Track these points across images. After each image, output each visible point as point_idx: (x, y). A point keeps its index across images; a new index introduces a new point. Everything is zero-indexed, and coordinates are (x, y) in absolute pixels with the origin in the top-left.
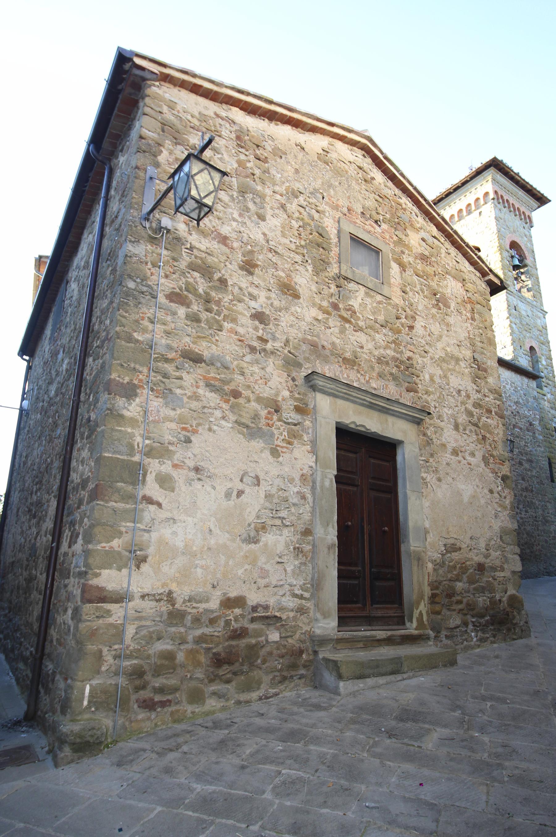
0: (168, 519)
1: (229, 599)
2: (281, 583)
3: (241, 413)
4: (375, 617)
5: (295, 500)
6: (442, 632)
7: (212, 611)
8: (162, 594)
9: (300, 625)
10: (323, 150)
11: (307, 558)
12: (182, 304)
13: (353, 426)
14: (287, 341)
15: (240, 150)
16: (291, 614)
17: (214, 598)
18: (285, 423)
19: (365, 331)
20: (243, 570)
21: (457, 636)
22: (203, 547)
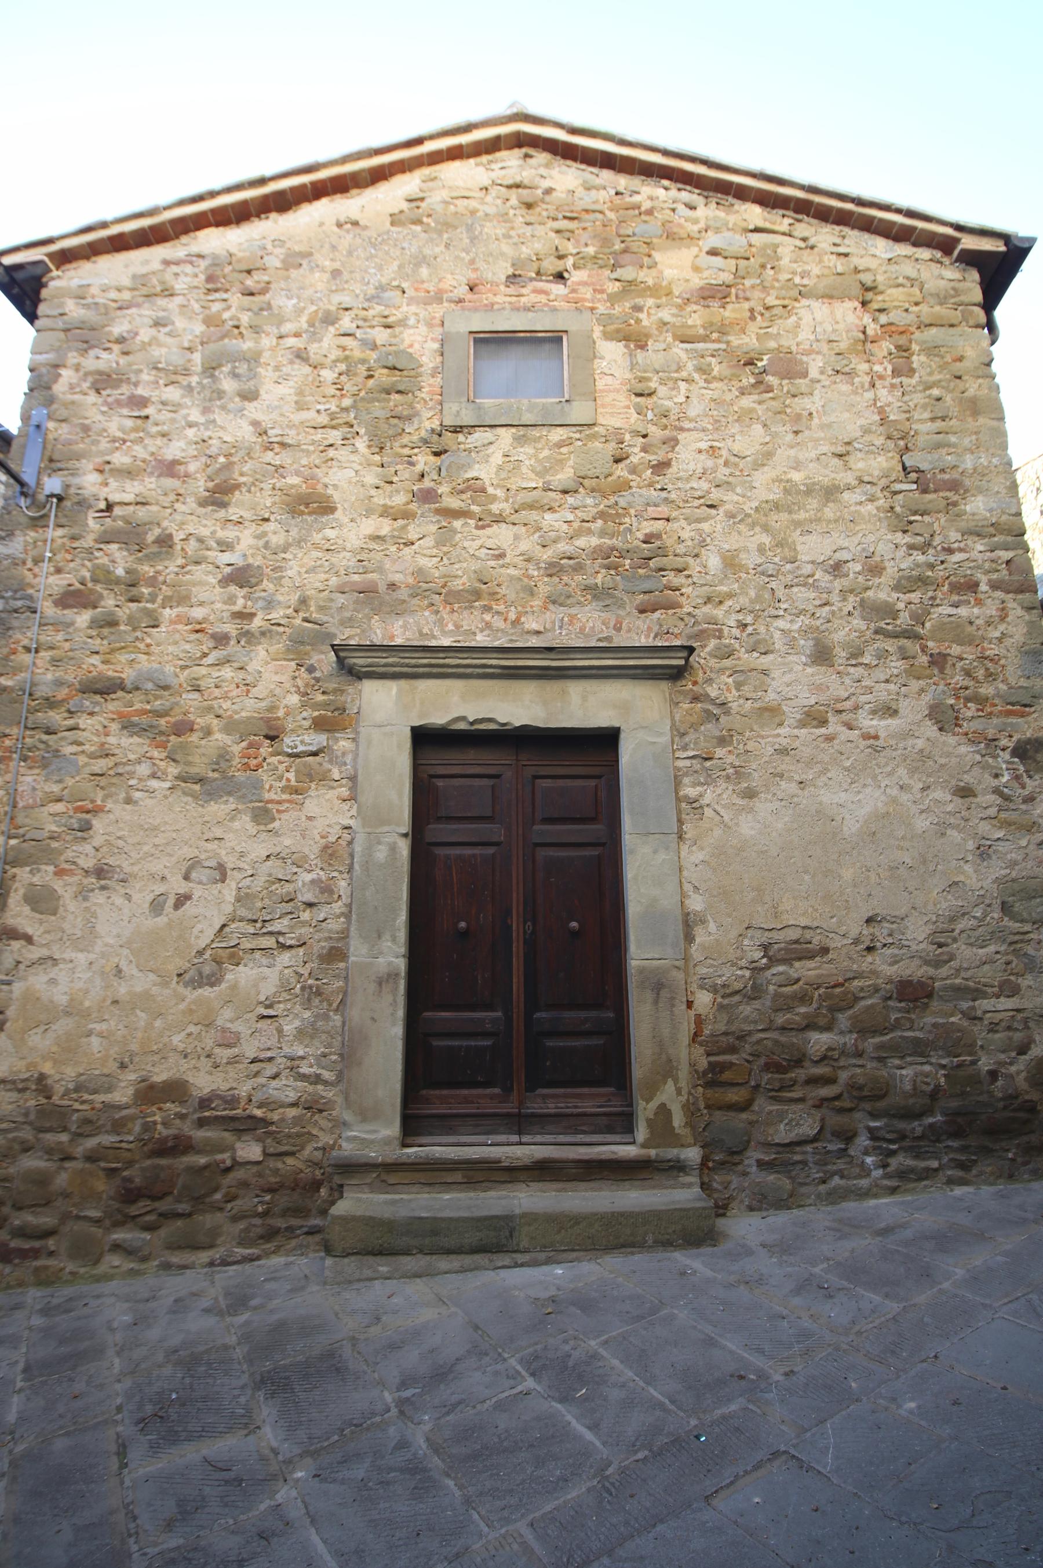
0: (41, 961)
1: (152, 1087)
2: (269, 1054)
3: (190, 758)
4: (533, 1115)
5: (309, 897)
6: (750, 1153)
7: (121, 1108)
8: (26, 1080)
9: (314, 1132)
10: (411, 201)
11: (330, 1005)
12: (85, 607)
13: (462, 726)
14: (304, 601)
15: (210, 298)
16: (292, 1112)
17: (123, 1084)
18: (290, 755)
19: (514, 518)
20: (183, 1034)
21: (804, 1163)
22: (104, 1000)
